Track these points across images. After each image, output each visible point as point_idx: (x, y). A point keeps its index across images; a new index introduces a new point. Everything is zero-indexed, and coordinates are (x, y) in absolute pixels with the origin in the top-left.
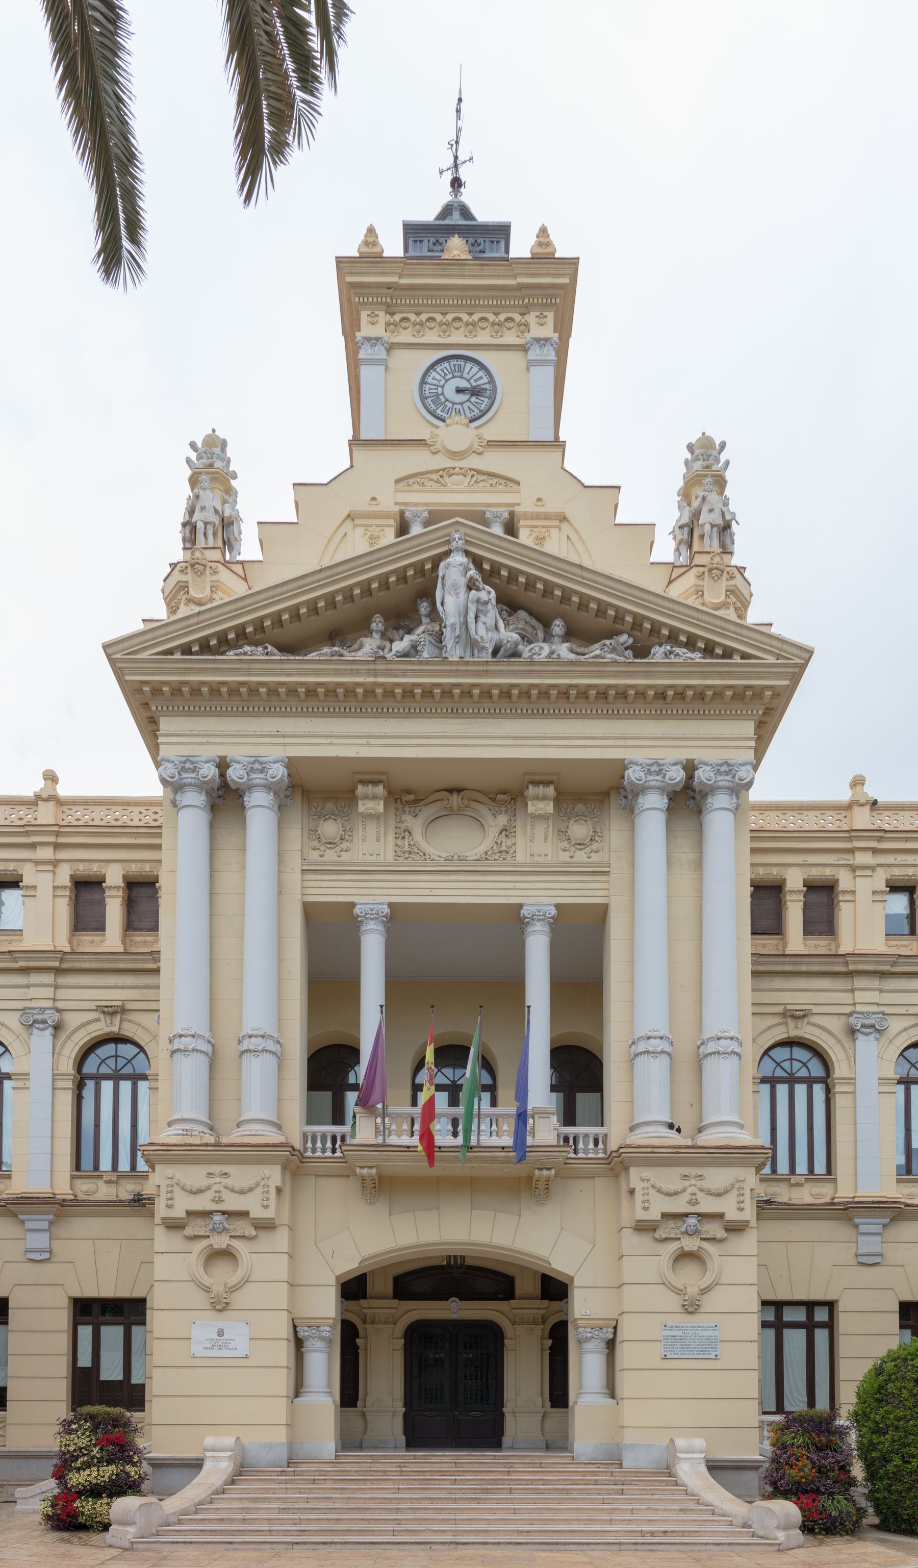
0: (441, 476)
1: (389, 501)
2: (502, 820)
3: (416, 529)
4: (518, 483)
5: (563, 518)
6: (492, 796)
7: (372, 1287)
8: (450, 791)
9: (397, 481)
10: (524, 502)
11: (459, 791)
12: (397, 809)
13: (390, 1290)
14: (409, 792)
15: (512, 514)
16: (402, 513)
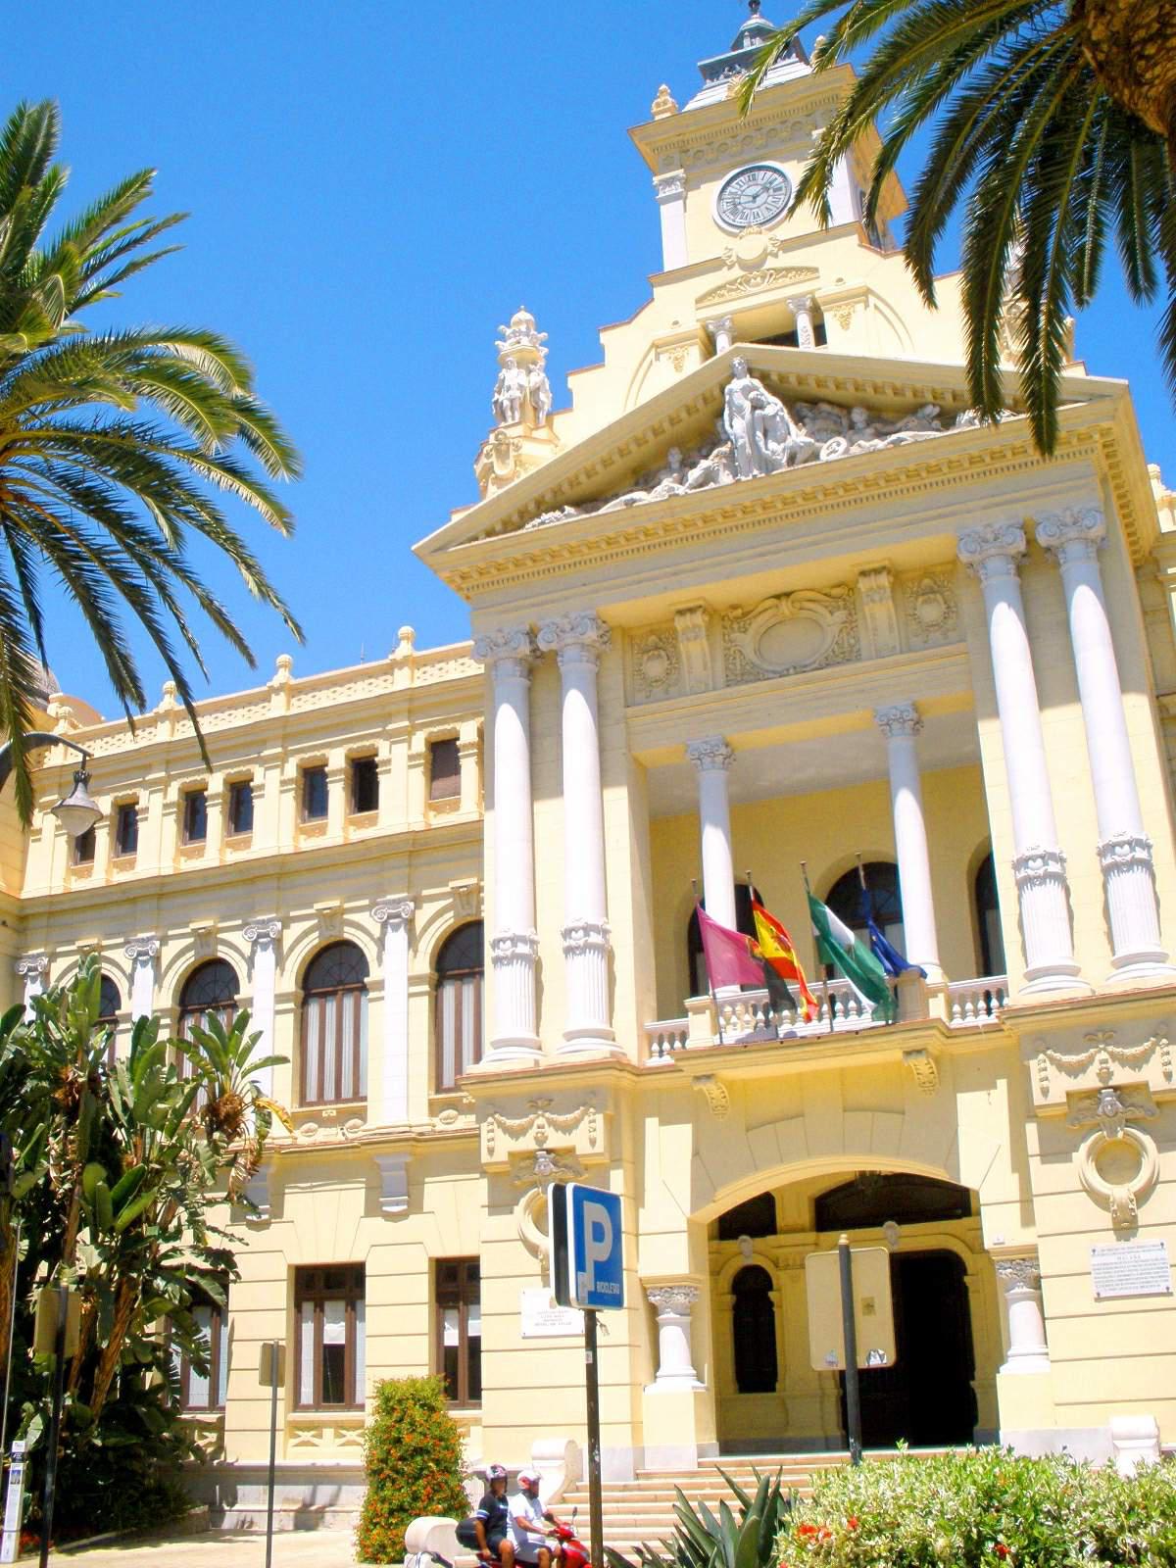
0: (740, 284)
1: (691, 321)
2: (841, 615)
3: (723, 343)
4: (816, 270)
5: (868, 292)
6: (827, 591)
7: (784, 1215)
8: (778, 597)
9: (699, 301)
10: (824, 287)
11: (788, 595)
12: (724, 627)
13: (805, 1215)
14: (734, 607)
15: (813, 300)
16: (705, 328)
